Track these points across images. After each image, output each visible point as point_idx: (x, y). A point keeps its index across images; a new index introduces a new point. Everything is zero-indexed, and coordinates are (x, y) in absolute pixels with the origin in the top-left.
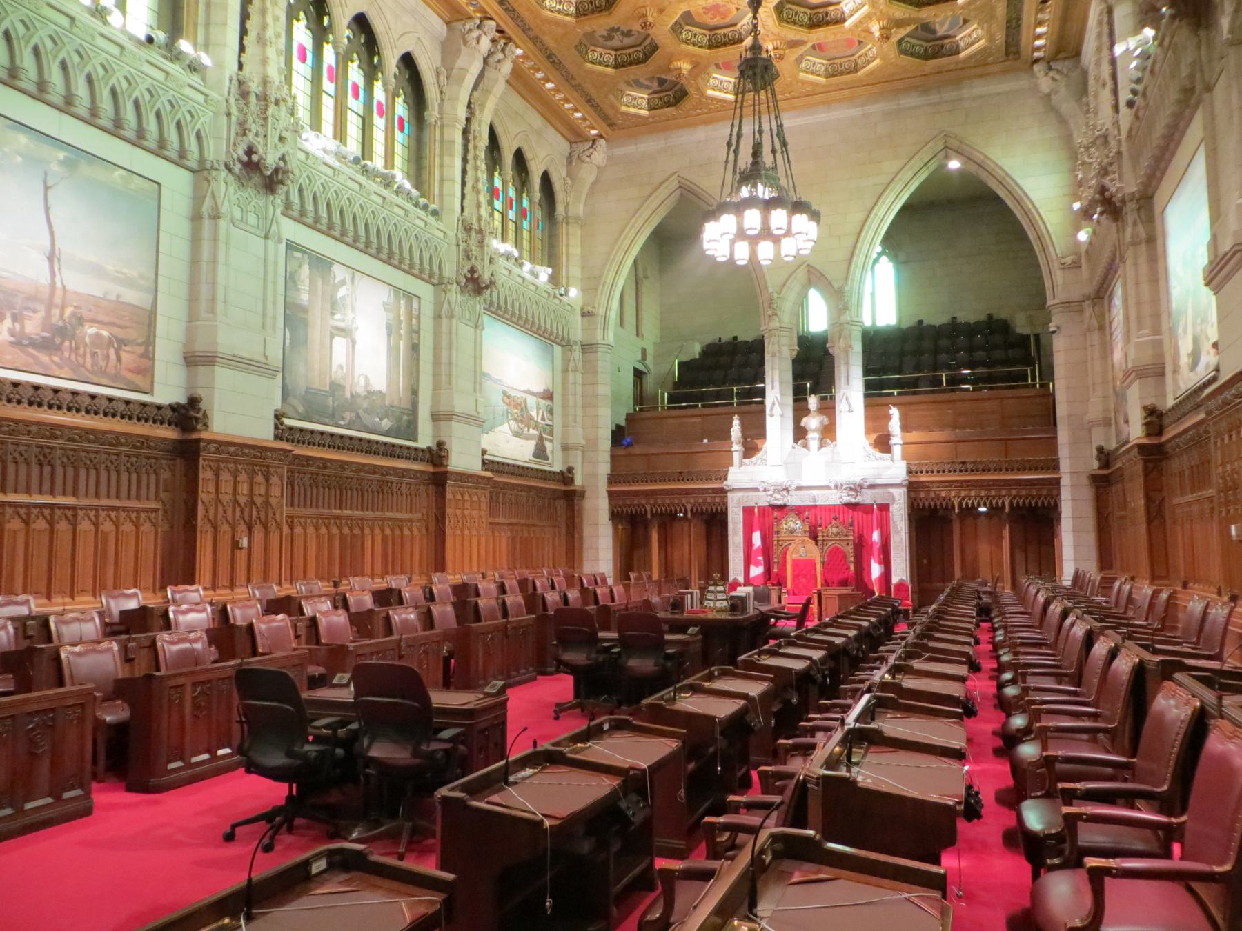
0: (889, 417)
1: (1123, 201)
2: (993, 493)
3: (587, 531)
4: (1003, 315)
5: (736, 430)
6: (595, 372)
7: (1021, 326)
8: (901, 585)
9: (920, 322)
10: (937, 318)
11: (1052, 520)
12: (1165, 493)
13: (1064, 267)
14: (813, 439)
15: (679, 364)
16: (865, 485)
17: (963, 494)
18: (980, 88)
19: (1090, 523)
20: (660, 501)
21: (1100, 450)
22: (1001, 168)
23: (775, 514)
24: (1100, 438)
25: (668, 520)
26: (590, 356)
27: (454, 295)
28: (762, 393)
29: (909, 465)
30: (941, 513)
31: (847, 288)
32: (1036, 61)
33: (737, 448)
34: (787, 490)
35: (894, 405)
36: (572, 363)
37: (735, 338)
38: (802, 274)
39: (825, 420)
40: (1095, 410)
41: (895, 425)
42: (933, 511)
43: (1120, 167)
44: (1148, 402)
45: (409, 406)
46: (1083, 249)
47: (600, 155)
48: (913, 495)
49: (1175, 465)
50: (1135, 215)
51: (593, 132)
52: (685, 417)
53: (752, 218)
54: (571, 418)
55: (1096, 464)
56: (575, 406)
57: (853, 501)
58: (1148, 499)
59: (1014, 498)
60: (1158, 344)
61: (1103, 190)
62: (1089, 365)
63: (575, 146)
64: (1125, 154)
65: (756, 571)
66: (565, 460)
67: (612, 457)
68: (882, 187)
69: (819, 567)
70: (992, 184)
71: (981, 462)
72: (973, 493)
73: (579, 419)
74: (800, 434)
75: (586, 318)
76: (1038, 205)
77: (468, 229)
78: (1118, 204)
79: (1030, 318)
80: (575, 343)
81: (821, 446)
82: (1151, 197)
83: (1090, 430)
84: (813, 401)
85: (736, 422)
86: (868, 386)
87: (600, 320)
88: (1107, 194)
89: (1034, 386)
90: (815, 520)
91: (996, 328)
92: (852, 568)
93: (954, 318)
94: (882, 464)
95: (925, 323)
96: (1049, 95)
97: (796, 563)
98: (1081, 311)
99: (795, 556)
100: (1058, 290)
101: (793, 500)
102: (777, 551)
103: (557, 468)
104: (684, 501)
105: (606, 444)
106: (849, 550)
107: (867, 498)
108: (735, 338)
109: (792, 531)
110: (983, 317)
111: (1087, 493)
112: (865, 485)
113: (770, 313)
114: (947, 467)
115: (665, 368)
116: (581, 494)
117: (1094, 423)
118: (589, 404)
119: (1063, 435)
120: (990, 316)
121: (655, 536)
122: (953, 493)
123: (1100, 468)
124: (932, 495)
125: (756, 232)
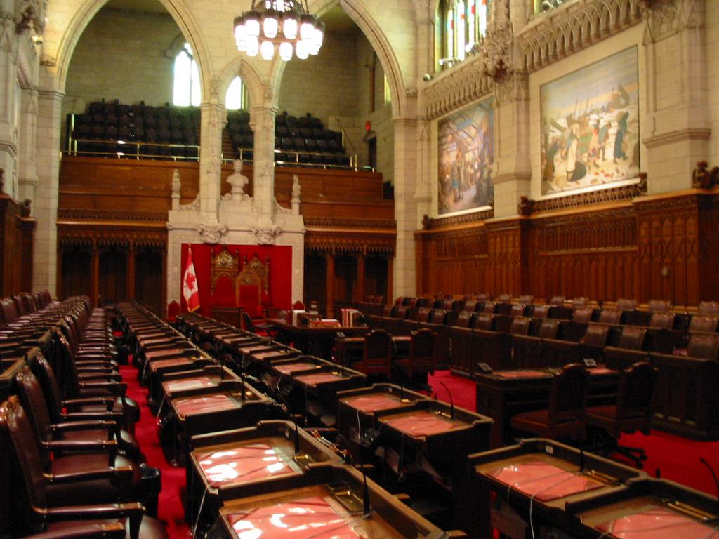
0: (291, 183)
3: (37, 258)
4: (316, 115)
6: (51, 118)
7: (332, 125)
11: (387, 261)
19: (412, 264)
20: (106, 236)
21: (426, 217)
23: (212, 251)
26: (46, 102)
29: (304, 218)
30: (320, 254)
31: (271, 83)
34: (219, 232)
35: (297, 174)
36: (31, 106)
37: (117, 101)
38: (236, 67)
40: (420, 192)
41: (296, 187)
42: (315, 252)
43: (512, 50)
44: (523, 194)
50: (520, 82)
53: (290, 25)
54: (28, 156)
57: (268, 243)
59: (369, 245)
60: (528, 161)
61: (501, 63)
64: (515, 45)
66: (21, 195)
67: (60, 194)
69: (260, 292)
72: (344, 241)
73: (34, 159)
74: (226, 189)
78: (508, 73)
79: (337, 120)
80: (35, 87)
81: (243, 200)
85: (176, 174)
88: (504, 67)
90: (242, 253)
93: (285, 113)
97: (243, 288)
99: (242, 283)
101: (225, 241)
103: (17, 199)
104: (128, 236)
105: (55, 184)
110: (304, 115)
111: (412, 244)
116: (32, 225)
117: (422, 200)
119: (400, 206)
120: (309, 115)
122: (331, 241)
123: (424, 229)
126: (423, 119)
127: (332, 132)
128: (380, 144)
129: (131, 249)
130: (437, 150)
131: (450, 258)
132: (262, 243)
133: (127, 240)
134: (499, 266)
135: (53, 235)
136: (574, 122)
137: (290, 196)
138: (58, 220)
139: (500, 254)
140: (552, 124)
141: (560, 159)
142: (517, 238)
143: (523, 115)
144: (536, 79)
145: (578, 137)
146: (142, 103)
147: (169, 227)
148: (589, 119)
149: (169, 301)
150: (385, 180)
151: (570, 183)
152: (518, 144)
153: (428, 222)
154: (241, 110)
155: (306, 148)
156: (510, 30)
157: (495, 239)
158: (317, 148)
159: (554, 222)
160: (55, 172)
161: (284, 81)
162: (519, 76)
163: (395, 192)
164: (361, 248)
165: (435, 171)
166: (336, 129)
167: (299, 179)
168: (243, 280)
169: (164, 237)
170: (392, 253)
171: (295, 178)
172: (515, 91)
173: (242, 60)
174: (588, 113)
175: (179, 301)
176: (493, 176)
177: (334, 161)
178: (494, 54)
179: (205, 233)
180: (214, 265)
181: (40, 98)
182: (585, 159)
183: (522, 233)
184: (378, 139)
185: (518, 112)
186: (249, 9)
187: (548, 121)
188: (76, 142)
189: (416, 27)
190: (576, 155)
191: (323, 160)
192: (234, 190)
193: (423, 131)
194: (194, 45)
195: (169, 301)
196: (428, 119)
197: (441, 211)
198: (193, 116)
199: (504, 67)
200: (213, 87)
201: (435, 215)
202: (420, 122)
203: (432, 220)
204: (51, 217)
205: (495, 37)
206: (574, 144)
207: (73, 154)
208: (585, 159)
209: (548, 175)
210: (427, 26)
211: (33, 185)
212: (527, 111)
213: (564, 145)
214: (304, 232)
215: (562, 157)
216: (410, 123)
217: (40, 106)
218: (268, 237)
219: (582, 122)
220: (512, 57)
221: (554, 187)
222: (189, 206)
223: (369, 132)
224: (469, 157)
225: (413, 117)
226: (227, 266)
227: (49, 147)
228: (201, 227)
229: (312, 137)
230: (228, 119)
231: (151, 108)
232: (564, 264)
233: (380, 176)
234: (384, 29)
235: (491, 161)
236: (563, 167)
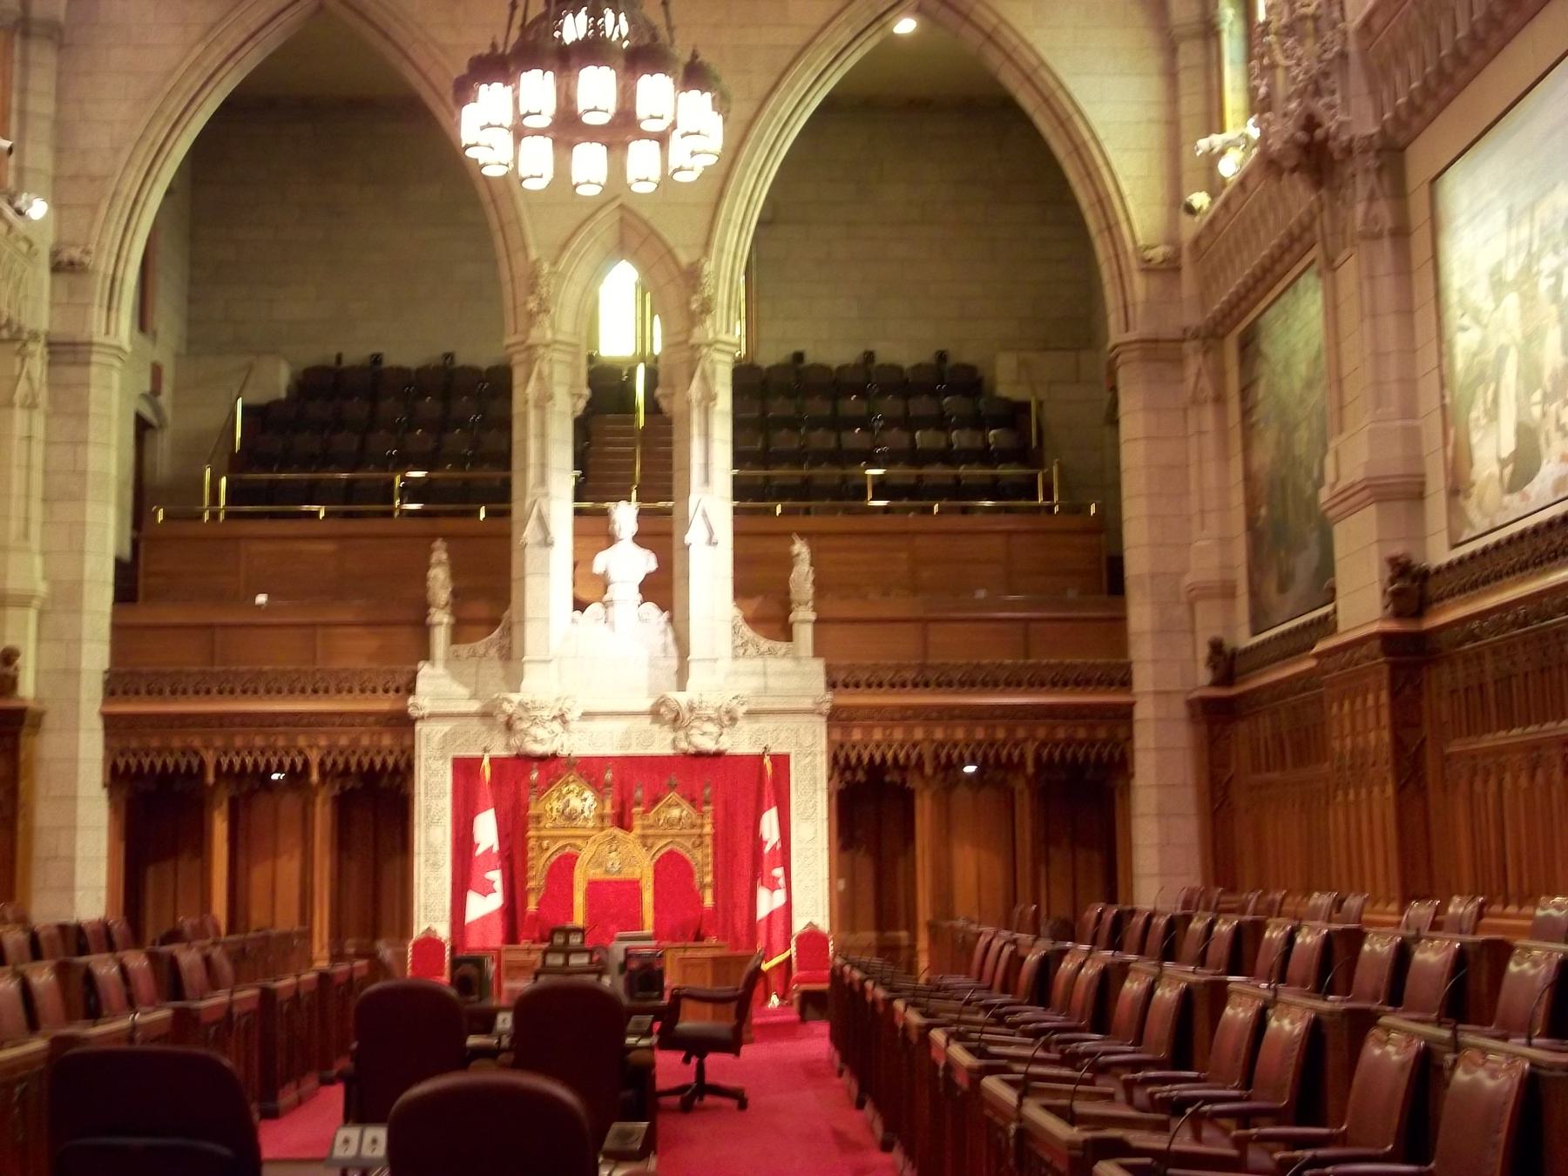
0: (788, 562)
1: (1348, 150)
2: (1001, 734)
4: (966, 355)
5: (439, 580)
6: (82, 416)
7: (1007, 383)
8: (812, 939)
9: (799, 357)
10: (832, 349)
12: (1426, 730)
13: (1148, 268)
15: (246, 410)
17: (939, 734)
19: (1187, 800)
21: (1216, 647)
22: (1030, 47)
24: (1209, 624)
25: (249, 787)
26: (71, 373)
28: (501, 496)
29: (829, 670)
30: (892, 777)
31: (709, 267)
33: (441, 619)
35: (802, 535)
36: (23, 387)
37: (377, 359)
39: (646, 562)
41: (802, 576)
42: (876, 770)
44: (1397, 549)
48: (837, 736)
49: (1441, 679)
50: (1373, 178)
52: (297, 538)
53: (597, 88)
55: (1204, 676)
56: (28, 496)
57: (709, 745)
58: (1398, 743)
60: (1412, 437)
61: (1310, 123)
62: (1193, 471)
65: (483, 905)
68: (788, 56)
69: (648, 897)
70: (1011, 81)
71: (978, 666)
73: (35, 530)
75: (64, 279)
76: (1101, 135)
78: (1337, 156)
80: (35, 336)
82: (1403, 149)
85: (440, 554)
86: (740, 490)
87: (100, 287)
88: (1319, 133)
89: (1050, 509)
90: (629, 784)
91: (950, 384)
92: (708, 901)
93: (869, 356)
94: (774, 665)
95: (810, 359)
98: (1179, 362)
99: (597, 874)
100: (1138, 313)
104: (302, 742)
106: (702, 862)
107: (741, 742)
108: (377, 359)
109: (571, 817)
110: (926, 356)
111: (1182, 736)
112: (741, 710)
113: (532, 305)
114: (909, 675)
115: (207, 419)
118: (64, 490)
119: (1140, 614)
120: (942, 356)
121: (220, 828)
123: (1215, 683)
124: (878, 735)
126: (1196, 336)
127: (1006, 401)
129: (315, 777)
131: (1275, 775)
132: (692, 750)
133: (301, 752)
134: (1351, 797)
135: (91, 748)
137: (786, 606)
138: (105, 701)
139: (1352, 752)
141: (1483, 421)
142: (1384, 697)
143: (1386, 287)
146: (449, 356)
147: (413, 712)
148: (1539, 273)
151: (1507, 499)
152: (1378, 384)
153: (1225, 663)
155: (915, 457)
156: (1336, 14)
157: (1341, 706)
158: (947, 456)
159: (1475, 638)
162: (1372, 162)
164: (1016, 753)
165: (1237, 497)
167: (811, 547)
168: (597, 861)
169: (407, 742)
170: (1119, 765)
171: (800, 548)
172: (1360, 209)
173: (621, 206)
175: (443, 931)
176: (1324, 494)
177: (993, 489)
178: (1288, 99)
179: (520, 726)
180: (538, 818)
181: (50, 364)
182: (1536, 411)
183: (1393, 680)
185: (1372, 277)
188: (224, 481)
189: (1170, 48)
192: (614, 592)
193: (1199, 375)
195: (419, 930)
196: (1211, 336)
197: (1258, 622)
201: (1244, 639)
202: (1189, 347)
203: (1235, 654)
204: (84, 696)
205: (1290, 42)
207: (214, 516)
210: (1198, 43)
212: (1404, 269)
214: (826, 707)
216: (1160, 351)
217: (53, 385)
218: (710, 727)
220: (1345, 99)
222: (480, 646)
225: (1170, 330)
226: (580, 823)
227: (79, 498)
228: (506, 706)
229: (941, 423)
230: (591, 384)
231: (472, 371)
232: (1508, 777)
236: (1491, 448)
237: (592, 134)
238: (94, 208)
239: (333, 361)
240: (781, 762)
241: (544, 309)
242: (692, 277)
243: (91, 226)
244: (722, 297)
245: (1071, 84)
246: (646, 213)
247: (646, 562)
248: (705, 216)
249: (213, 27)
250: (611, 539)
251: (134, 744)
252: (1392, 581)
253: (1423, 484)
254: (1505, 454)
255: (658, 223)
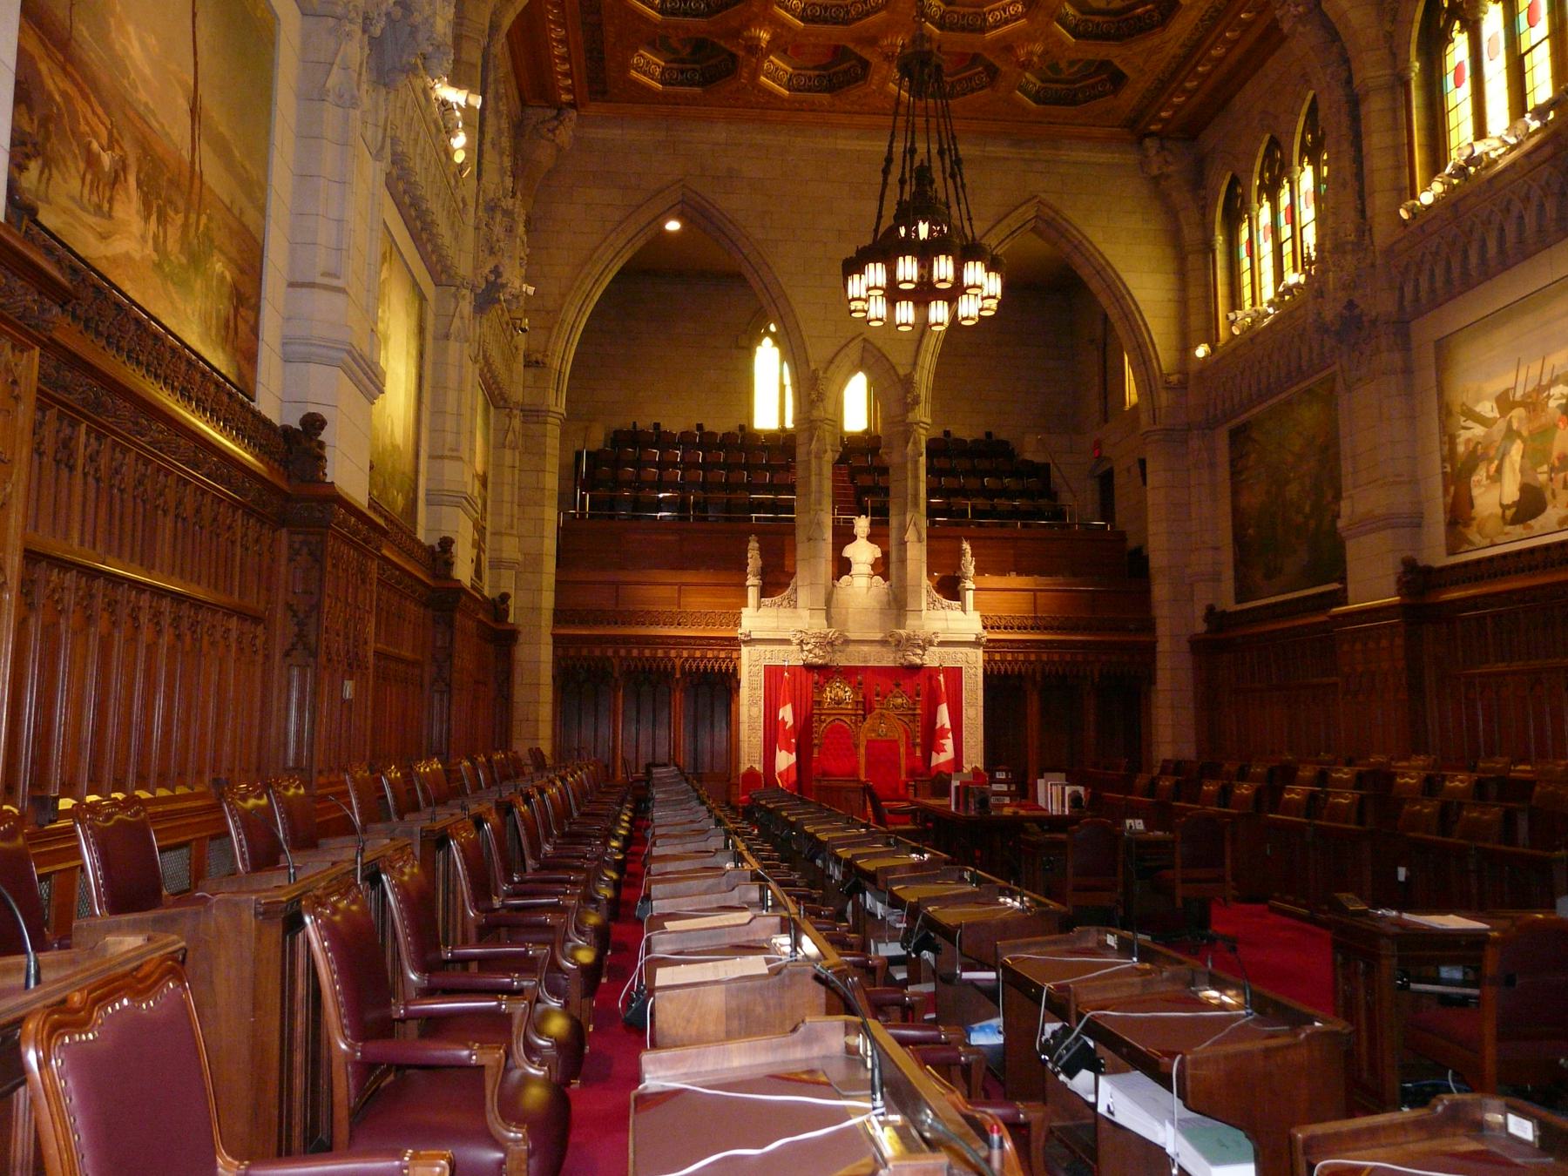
0: (960, 554)
1: (1374, 322)
3: (520, 694)
5: (754, 559)
7: (1031, 452)
13: (1169, 387)
14: (861, 574)
16: (936, 641)
18: (1081, 154)
27: (466, 307)
29: (984, 618)
31: (917, 377)
32: (1151, 134)
33: (752, 581)
34: (831, 644)
36: (510, 435)
39: (873, 551)
41: (969, 564)
45: (412, 475)
46: (1193, 368)
47: (565, 135)
51: (565, 97)
54: (506, 520)
55: (1201, 627)
57: (918, 661)
61: (1351, 305)
63: (529, 111)
67: (557, 581)
69: (902, 750)
70: (1085, 273)
75: (533, 370)
77: (492, 208)
83: (1191, 585)
84: (862, 524)
88: (1357, 311)
92: (918, 754)
93: (947, 433)
96: (1155, 178)
97: (870, 743)
101: (842, 660)
102: (820, 729)
104: (673, 653)
105: (550, 565)
106: (917, 728)
107: (932, 658)
110: (979, 434)
112: (936, 641)
119: (1161, 591)
120: (989, 435)
125: (911, 286)
128: (1119, 479)
130: (1228, 483)
133: (670, 659)
135: (546, 653)
136: (1514, 405)
140: (1463, 414)
141: (1485, 482)
142: (1399, 641)
144: (1426, 331)
145: (1525, 433)
148: (1549, 397)
149: (744, 768)
150: (1132, 544)
151: (1508, 528)
154: (866, 432)
155: (984, 492)
160: (550, 545)
161: (938, 375)
163: (1151, 565)
165: (1226, 525)
166: (1039, 459)
171: (966, 546)
174: (1544, 383)
175: (759, 767)
176: (1340, 524)
180: (819, 703)
182: (1543, 478)
184: (1116, 471)
186: (868, 241)
187: (1457, 409)
190: (1522, 471)
191: (1015, 513)
192: (855, 569)
194: (781, 323)
195: (744, 768)
197: (1241, 596)
198: (782, 447)
199: (1357, 311)
200: (813, 390)
201: (1229, 604)
206: (1516, 451)
208: (1543, 478)
209: (1459, 514)
211: (511, 568)
213: (1492, 453)
215: (1488, 477)
219: (1533, 403)
221: (1473, 534)
222: (777, 599)
223: (1100, 458)
224: (1293, 491)
227: (540, 504)
233: (1122, 537)
234: (1120, 267)
235: (1338, 497)
236: (1493, 495)
237: (906, 296)
238: (550, 329)
239: (630, 427)
240: (955, 674)
241: (821, 397)
242: (907, 383)
243: (548, 341)
244: (923, 398)
245: (1125, 277)
246: (879, 343)
247: (873, 551)
248: (911, 348)
249: (621, 223)
250: (853, 538)
251: (572, 652)
252: (1404, 573)
253: (1421, 516)
254: (1507, 500)
255: (886, 350)
